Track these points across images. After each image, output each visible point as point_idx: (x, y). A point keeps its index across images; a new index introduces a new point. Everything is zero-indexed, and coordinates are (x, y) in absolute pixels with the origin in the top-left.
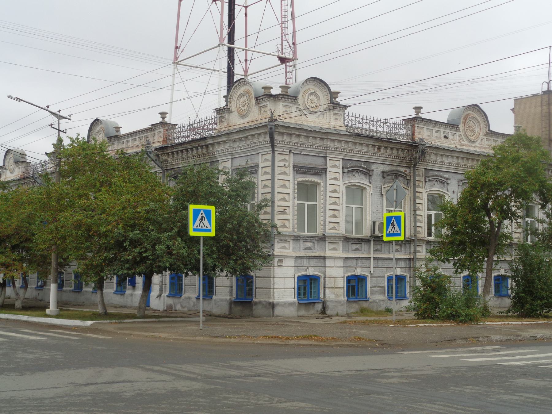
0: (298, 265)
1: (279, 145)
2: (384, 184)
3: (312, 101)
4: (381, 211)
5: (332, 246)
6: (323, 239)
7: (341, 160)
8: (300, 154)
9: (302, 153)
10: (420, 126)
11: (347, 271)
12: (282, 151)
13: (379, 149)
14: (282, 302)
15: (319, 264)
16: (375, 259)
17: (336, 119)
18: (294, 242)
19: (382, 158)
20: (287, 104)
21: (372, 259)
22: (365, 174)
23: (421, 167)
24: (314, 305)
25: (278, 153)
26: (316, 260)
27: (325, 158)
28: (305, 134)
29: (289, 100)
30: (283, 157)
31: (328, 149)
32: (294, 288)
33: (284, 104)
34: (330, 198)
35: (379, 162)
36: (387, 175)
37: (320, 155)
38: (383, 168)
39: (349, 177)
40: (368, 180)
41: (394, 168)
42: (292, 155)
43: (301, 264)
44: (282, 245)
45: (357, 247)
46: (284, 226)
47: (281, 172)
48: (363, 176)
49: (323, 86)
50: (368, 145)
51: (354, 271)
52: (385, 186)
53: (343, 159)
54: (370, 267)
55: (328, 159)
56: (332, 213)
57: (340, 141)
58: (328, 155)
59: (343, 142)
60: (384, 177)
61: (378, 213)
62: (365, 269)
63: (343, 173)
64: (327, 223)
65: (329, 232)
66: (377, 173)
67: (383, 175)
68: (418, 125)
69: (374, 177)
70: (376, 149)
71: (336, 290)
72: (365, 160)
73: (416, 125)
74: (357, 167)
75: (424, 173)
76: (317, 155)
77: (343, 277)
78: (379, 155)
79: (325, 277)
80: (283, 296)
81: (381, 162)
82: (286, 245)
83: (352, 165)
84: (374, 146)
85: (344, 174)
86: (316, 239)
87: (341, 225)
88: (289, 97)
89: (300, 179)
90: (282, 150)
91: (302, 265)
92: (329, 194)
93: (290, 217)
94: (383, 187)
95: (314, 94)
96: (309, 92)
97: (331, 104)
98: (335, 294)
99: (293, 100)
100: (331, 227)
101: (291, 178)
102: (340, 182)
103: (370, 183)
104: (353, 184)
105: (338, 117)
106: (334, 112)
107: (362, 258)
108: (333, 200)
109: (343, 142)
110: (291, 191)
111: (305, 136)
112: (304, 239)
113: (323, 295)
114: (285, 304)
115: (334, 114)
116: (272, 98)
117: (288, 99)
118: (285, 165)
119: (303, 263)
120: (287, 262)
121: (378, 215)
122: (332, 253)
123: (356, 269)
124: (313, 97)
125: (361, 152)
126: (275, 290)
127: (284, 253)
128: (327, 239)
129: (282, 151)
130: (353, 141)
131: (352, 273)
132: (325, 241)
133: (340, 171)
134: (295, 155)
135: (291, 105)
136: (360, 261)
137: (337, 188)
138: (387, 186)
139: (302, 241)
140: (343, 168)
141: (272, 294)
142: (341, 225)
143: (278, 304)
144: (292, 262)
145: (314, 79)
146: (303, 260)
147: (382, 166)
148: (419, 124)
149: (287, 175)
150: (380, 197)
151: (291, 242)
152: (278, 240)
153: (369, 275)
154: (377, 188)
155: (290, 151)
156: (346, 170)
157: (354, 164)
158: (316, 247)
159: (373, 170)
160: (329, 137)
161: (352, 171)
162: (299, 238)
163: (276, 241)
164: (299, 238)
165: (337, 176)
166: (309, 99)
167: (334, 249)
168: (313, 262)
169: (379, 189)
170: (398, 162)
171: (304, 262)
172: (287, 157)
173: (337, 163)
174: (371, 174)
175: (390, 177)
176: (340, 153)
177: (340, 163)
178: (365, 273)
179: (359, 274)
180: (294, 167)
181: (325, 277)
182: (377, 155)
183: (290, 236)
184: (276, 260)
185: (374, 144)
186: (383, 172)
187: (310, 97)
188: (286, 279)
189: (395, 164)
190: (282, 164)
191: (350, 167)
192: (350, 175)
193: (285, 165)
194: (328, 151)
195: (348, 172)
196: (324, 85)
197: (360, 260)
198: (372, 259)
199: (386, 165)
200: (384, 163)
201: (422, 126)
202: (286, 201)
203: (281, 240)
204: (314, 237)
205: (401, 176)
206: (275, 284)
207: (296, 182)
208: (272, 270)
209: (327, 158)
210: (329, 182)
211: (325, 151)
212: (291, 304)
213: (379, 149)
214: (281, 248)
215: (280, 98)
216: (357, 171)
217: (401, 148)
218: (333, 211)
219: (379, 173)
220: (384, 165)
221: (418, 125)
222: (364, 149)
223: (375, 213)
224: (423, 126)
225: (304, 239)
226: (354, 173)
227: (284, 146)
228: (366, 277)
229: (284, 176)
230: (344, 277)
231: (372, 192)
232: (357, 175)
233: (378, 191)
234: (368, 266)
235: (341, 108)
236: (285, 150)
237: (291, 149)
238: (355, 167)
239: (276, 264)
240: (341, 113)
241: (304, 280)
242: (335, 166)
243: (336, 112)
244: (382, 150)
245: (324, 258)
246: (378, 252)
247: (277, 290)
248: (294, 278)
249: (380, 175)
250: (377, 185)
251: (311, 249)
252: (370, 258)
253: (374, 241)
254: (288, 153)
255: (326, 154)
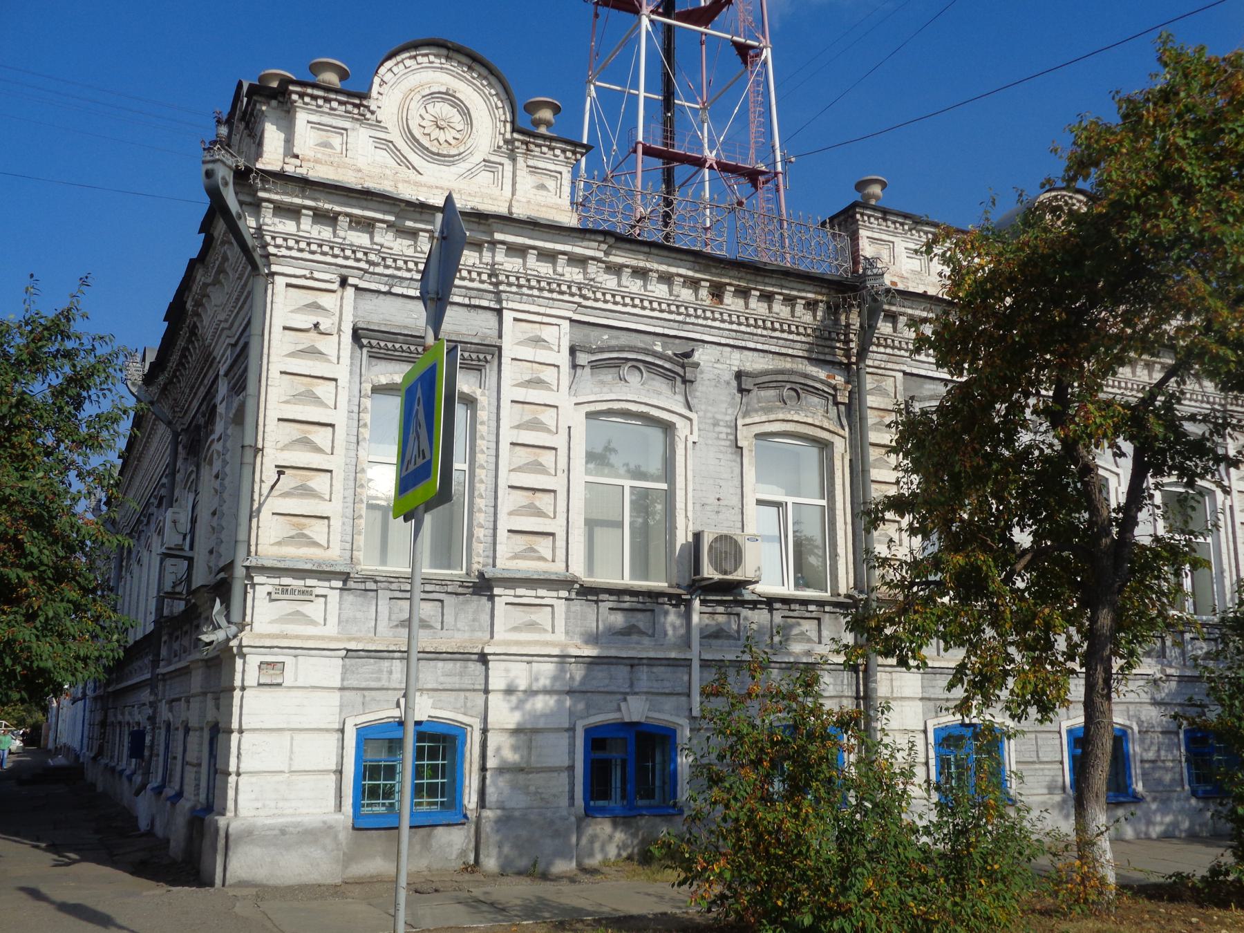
0: (363, 685)
1: (284, 252)
2: (744, 416)
3: (440, 123)
4: (735, 501)
5: (521, 616)
6: (483, 586)
7: (566, 324)
8: (389, 293)
9: (396, 290)
10: (876, 235)
11: (588, 707)
12: (304, 277)
13: (717, 292)
14: (271, 828)
15: (467, 682)
16: (705, 664)
17: (542, 187)
18: (349, 597)
19: (734, 327)
20: (326, 119)
21: (696, 665)
22: (669, 375)
23: (890, 366)
24: (429, 835)
25: (288, 285)
26: (450, 665)
27: (499, 312)
28: (391, 218)
29: (335, 104)
30: (310, 297)
31: (502, 278)
32: (340, 772)
33: (314, 118)
34: (518, 448)
35: (723, 341)
36: (760, 386)
37: (473, 302)
38: (737, 361)
39: (602, 383)
40: (681, 398)
41: (787, 364)
42: (350, 291)
43: (379, 679)
44: (285, 607)
45: (633, 621)
46: (303, 539)
47: (300, 347)
48: (660, 384)
49: (485, 78)
50: (666, 279)
51: (619, 709)
52: (748, 421)
53: (571, 320)
54: (689, 695)
55: (508, 316)
56: (521, 498)
57: (549, 256)
58: (505, 304)
59: (562, 260)
60: (741, 390)
61: (723, 509)
62: (669, 703)
63: (574, 366)
64: (502, 534)
65: (507, 563)
66: (718, 376)
67: (739, 384)
68: (869, 234)
69: (703, 388)
70: (704, 292)
71: (537, 780)
72: (667, 331)
73: (863, 233)
74: (632, 349)
75: (900, 388)
76: (467, 301)
77: (567, 730)
78: (717, 316)
79: (485, 731)
80: (281, 804)
81: (731, 342)
82: (306, 608)
83: (614, 343)
84: (694, 284)
85: (579, 371)
86: (450, 589)
87: (561, 543)
88: (333, 96)
89: (384, 380)
90: (307, 273)
91: (384, 683)
92: (507, 436)
93: (334, 509)
94: (740, 422)
95: (448, 96)
96: (427, 92)
97: (516, 135)
98: (528, 794)
99: (350, 107)
100: (518, 549)
101: (342, 372)
102: (563, 398)
103: (690, 408)
104: (616, 406)
105: (551, 184)
106: (531, 163)
107: (652, 662)
108: (524, 455)
109: (562, 260)
110: (340, 418)
111: (390, 225)
112: (394, 586)
113: (474, 798)
114: (283, 832)
115: (534, 170)
116: (274, 103)
117: (327, 100)
118: (316, 326)
119: (385, 676)
120: (301, 670)
121: (721, 516)
122: (518, 643)
123: (625, 700)
124: (444, 110)
125: (643, 301)
126: (243, 779)
127: (297, 637)
128: (497, 591)
129: (304, 277)
130: (600, 255)
131: (610, 717)
132: (491, 598)
133: (564, 359)
134: (369, 295)
135: (347, 125)
136: (643, 673)
137: (547, 417)
138: (757, 419)
139: (384, 595)
140: (573, 351)
141: (231, 793)
142: (561, 543)
143: (249, 834)
144: (329, 671)
145: (444, 52)
146: (386, 663)
147: (736, 354)
148: (871, 229)
149: (329, 361)
150: (729, 456)
151: (334, 596)
152: (270, 589)
153: (684, 722)
154: (716, 424)
155: (344, 282)
156: (583, 358)
157: (624, 339)
158: (449, 618)
159: (697, 365)
160: (498, 236)
161: (615, 364)
162: (373, 586)
163: (261, 592)
164: (373, 586)
165: (548, 375)
166: (426, 116)
167: (532, 626)
168: (431, 674)
169: (725, 430)
170: (798, 345)
171: (391, 672)
172: (327, 300)
173: (548, 333)
174: (689, 376)
175: (772, 393)
176: (555, 295)
177: (560, 336)
178: (666, 714)
179: (635, 719)
180: (357, 335)
181: (485, 731)
182: (709, 314)
183: (324, 575)
184: (253, 660)
185: (690, 273)
186: (739, 375)
187: (429, 107)
188: (299, 737)
189: (790, 352)
190: (305, 321)
191: (601, 350)
192: (608, 376)
193: (316, 326)
194: (501, 288)
195: (595, 366)
196: (485, 72)
197: (645, 669)
198: (696, 665)
199: (756, 354)
200: (743, 344)
201: (884, 237)
202: (318, 450)
203: (285, 592)
204: (441, 582)
205: (816, 392)
206: (243, 758)
207: (368, 387)
208: (236, 701)
209: (505, 312)
210: (508, 393)
211: (491, 288)
212: (310, 835)
213: (717, 292)
214: (284, 619)
215: (295, 97)
216: (636, 365)
217: (804, 294)
218: (530, 494)
219: (728, 376)
220: (746, 353)
221: (869, 234)
222: (660, 290)
223: (708, 508)
224: (891, 238)
225: (394, 586)
226: (625, 369)
227: (306, 255)
228: (674, 731)
229: (310, 363)
230: (572, 729)
231: (691, 439)
232: (634, 378)
233: (723, 436)
234: (679, 690)
235: (558, 152)
236: (316, 275)
237: (345, 272)
238: (621, 350)
239: (251, 680)
240: (559, 168)
241: (391, 741)
242: (537, 341)
243: (541, 164)
244: (728, 299)
245: (483, 658)
246: (719, 642)
247: (254, 779)
248: (342, 731)
249: (728, 383)
250: (719, 417)
251: (430, 627)
252: (687, 663)
253: (703, 602)
254: (335, 286)
255: (499, 301)
